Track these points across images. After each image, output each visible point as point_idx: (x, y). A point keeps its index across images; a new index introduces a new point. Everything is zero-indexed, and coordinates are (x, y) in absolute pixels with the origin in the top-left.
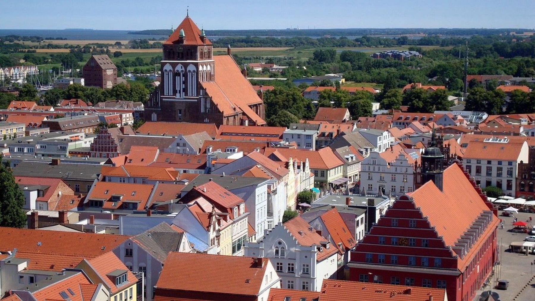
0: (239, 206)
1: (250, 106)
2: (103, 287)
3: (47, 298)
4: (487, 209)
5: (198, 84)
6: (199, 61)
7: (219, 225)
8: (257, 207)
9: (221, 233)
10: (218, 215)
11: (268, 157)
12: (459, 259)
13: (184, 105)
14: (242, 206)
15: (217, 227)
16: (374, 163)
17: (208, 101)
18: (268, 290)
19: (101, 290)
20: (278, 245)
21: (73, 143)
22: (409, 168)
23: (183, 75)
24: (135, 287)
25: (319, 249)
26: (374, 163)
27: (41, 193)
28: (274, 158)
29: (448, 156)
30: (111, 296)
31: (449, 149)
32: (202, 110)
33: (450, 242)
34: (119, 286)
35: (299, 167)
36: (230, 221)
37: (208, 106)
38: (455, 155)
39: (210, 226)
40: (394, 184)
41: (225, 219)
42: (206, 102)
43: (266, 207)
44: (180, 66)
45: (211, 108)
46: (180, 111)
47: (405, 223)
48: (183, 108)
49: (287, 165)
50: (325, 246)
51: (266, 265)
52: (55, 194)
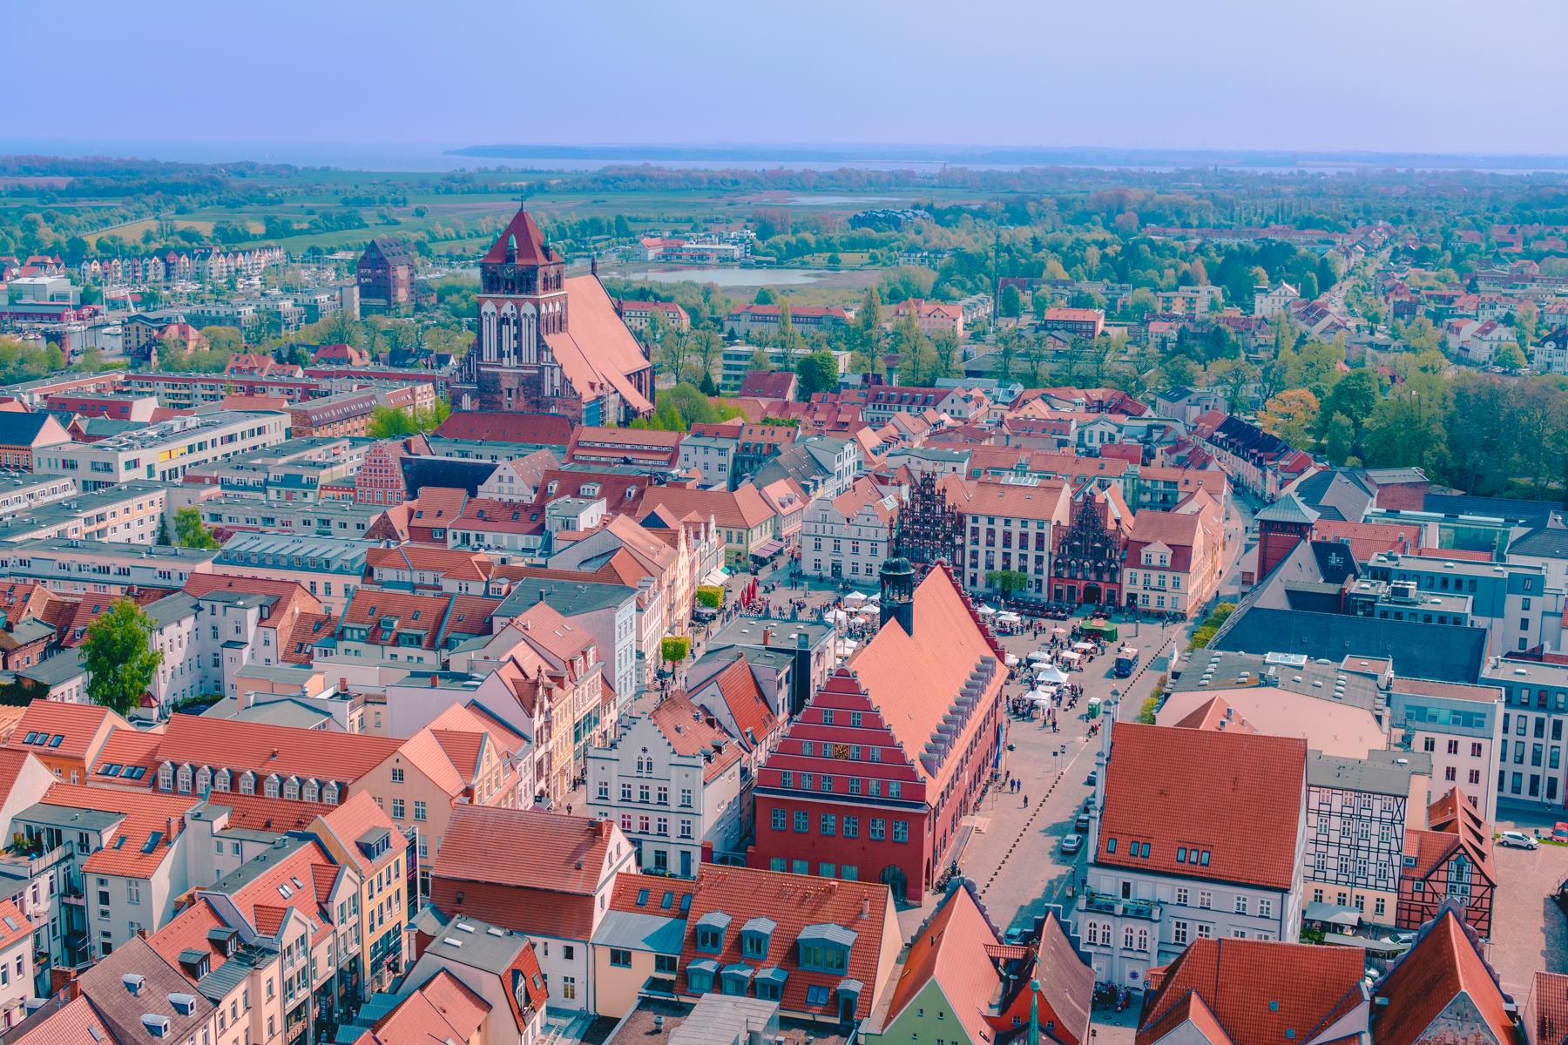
0: (584, 654)
1: (628, 377)
2: (348, 871)
4: (989, 653)
5: (540, 339)
6: (542, 296)
7: (550, 699)
8: (617, 648)
9: (553, 713)
11: (642, 524)
12: (929, 779)
13: (516, 381)
14: (591, 653)
15: (547, 705)
16: (824, 521)
17: (557, 371)
18: (614, 878)
20: (641, 754)
21: (327, 471)
22: (880, 530)
23: (515, 323)
25: (708, 759)
26: (824, 521)
27: (266, 611)
28: (653, 522)
29: (943, 508)
30: (362, 882)
31: (944, 497)
32: (547, 392)
33: (913, 752)
35: (697, 535)
36: (568, 685)
37: (557, 383)
38: (954, 507)
39: (534, 706)
40: (855, 559)
41: (561, 686)
43: (634, 642)
44: (508, 305)
45: (562, 386)
46: (510, 390)
49: (673, 542)
50: (718, 749)
51: (609, 834)
52: (288, 611)
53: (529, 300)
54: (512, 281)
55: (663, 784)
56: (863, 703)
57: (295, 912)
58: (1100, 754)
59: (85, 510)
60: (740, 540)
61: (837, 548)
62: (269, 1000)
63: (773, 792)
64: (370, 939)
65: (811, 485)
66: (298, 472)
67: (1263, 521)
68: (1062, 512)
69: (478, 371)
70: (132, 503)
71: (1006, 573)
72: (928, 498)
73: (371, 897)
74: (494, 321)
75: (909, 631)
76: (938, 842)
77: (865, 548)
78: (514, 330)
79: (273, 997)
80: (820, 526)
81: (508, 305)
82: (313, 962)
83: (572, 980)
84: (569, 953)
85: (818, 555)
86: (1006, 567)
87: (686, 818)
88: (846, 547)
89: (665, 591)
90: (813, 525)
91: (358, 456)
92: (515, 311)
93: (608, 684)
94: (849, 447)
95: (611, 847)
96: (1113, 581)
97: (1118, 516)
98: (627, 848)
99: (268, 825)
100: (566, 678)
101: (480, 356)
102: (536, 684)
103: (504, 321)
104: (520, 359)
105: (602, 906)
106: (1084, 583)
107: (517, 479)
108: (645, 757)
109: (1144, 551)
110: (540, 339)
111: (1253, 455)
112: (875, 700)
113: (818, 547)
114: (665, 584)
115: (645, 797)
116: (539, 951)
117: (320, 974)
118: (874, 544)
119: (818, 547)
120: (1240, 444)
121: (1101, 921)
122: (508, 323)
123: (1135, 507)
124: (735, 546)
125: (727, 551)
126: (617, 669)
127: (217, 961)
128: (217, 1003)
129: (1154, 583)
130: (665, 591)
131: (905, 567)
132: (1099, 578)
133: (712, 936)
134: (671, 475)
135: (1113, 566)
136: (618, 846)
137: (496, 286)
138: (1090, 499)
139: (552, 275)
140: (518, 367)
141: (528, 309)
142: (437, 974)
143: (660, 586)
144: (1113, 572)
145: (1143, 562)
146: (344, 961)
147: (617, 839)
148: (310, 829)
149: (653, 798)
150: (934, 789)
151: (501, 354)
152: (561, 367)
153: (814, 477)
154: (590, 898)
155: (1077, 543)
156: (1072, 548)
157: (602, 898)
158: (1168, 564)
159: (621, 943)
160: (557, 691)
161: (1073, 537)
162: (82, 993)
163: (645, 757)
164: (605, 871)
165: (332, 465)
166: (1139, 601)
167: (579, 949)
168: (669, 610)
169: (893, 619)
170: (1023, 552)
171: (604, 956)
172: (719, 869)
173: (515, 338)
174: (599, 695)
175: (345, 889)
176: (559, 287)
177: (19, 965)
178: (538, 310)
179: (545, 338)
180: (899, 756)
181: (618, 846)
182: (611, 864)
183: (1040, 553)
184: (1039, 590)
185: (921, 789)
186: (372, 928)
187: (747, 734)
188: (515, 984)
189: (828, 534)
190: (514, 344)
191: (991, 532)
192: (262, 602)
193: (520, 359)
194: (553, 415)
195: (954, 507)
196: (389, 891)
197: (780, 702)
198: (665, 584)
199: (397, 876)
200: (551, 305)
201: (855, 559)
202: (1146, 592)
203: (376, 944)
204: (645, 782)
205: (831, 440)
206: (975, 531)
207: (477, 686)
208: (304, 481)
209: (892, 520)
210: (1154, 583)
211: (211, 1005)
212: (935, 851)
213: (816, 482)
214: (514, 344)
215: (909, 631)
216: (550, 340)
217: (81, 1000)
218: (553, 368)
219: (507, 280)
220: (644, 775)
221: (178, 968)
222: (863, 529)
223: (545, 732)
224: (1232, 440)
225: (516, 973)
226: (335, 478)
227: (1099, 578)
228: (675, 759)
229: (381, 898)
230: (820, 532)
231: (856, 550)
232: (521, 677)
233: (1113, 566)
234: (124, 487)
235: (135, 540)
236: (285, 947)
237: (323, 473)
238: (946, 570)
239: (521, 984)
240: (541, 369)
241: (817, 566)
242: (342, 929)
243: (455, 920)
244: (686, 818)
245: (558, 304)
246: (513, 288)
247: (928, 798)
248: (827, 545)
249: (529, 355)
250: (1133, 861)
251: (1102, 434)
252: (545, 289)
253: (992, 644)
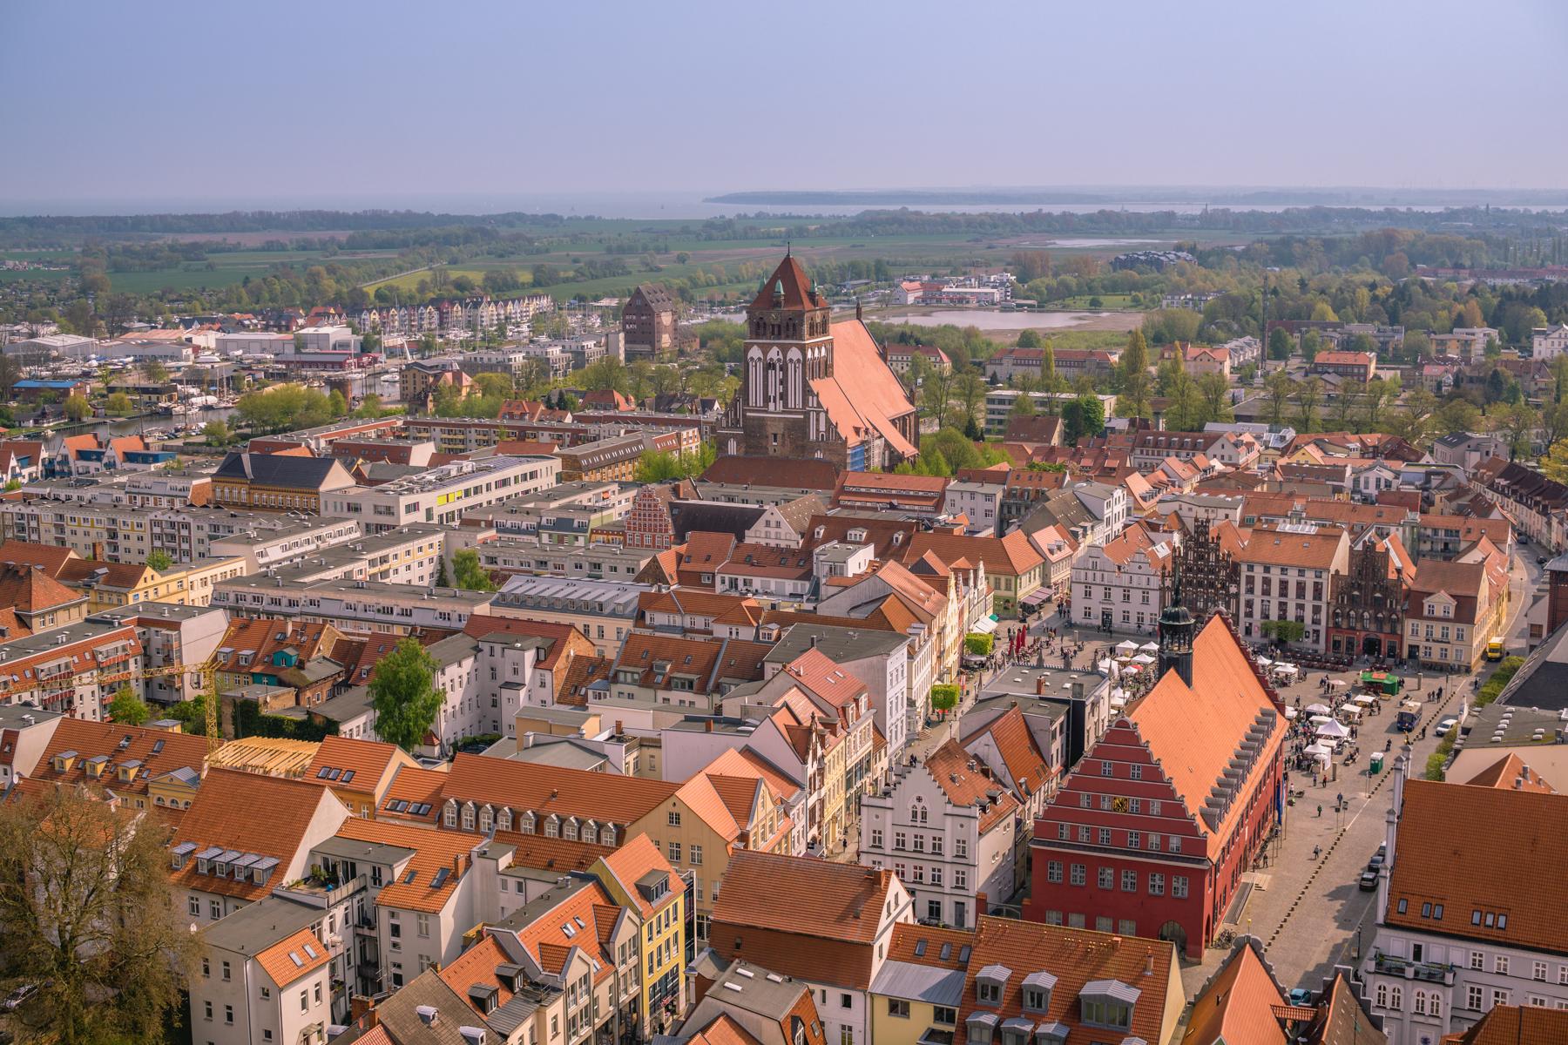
0: (856, 701)
1: (893, 422)
2: (629, 912)
3: (541, 940)
4: (1270, 706)
5: (805, 385)
7: (823, 746)
8: (889, 695)
9: (826, 760)
10: (822, 724)
14: (863, 700)
15: (819, 752)
17: (822, 416)
19: (626, 919)
20: (916, 803)
21: (598, 515)
22: (1152, 578)
24: (680, 900)
25: (984, 809)
27: (542, 652)
28: (922, 569)
29: (1217, 557)
30: (642, 924)
31: (1218, 545)
32: (813, 436)
33: (1194, 805)
34: (655, 904)
35: (966, 582)
36: (841, 733)
37: (822, 428)
38: (1229, 555)
39: (807, 753)
40: (1126, 607)
41: (834, 733)
42: (818, 420)
43: (905, 690)
44: (775, 349)
45: (827, 430)
46: (775, 435)
47: (1121, 772)
48: (779, 429)
49: (943, 587)
50: (993, 800)
51: (887, 884)
52: (564, 654)
54: (779, 326)
55: (938, 834)
56: (1144, 755)
57: (579, 952)
58: (1391, 812)
59: (369, 552)
60: (1008, 588)
61: (1107, 596)
62: (554, 1037)
63: (1050, 844)
64: (649, 980)
65: (1080, 531)
66: (571, 517)
67: (1553, 572)
68: (1340, 560)
69: (744, 416)
70: (413, 546)
71: (1282, 623)
72: (1202, 545)
73: (650, 939)
74: (760, 366)
75: (1188, 682)
76: (1218, 899)
77: (1136, 596)
78: (780, 375)
79: (557, 1034)
80: (1090, 574)
81: (775, 349)
82: (595, 1001)
83: (850, 1029)
84: (847, 1002)
85: (1088, 603)
86: (1283, 617)
87: (961, 868)
88: (1117, 595)
89: (934, 638)
90: (1083, 572)
91: (627, 500)
92: (781, 356)
93: (879, 731)
94: (1118, 493)
95: (890, 897)
96: (1393, 632)
97: (1399, 565)
98: (905, 898)
99: (550, 866)
100: (839, 725)
101: (746, 401)
102: (809, 731)
103: (770, 366)
104: (785, 405)
105: (881, 957)
106: (1363, 634)
107: (784, 522)
108: (919, 806)
109: (1427, 602)
110: (805, 385)
111: (1537, 503)
112: (1156, 752)
113: (1088, 594)
114: (935, 631)
115: (919, 846)
116: (817, 998)
117: (601, 1014)
118: (1145, 591)
119: (1088, 594)
120: (1524, 491)
121: (1391, 984)
122: (774, 368)
123: (1416, 555)
124: (1003, 593)
125: (995, 598)
126: (888, 716)
127: (504, 996)
128: (505, 1037)
129: (1437, 634)
130: (934, 638)
131: (1185, 617)
132: (1380, 630)
133: (993, 989)
134: (938, 521)
135: (1394, 617)
136: (897, 895)
137: (762, 330)
138: (1370, 548)
139: (818, 320)
140: (783, 412)
141: (794, 354)
142: (718, 1018)
143: (930, 633)
144: (1394, 623)
145: (1426, 613)
146: (624, 998)
147: (895, 887)
148: (592, 870)
149: (928, 848)
150: (1216, 843)
151: (767, 399)
152: (827, 412)
153: (1082, 524)
154: (871, 947)
155: (1356, 593)
156: (1352, 599)
157: (881, 947)
158: (1452, 615)
159: (899, 993)
160: (830, 738)
161: (1352, 586)
162: (380, 1022)
163: (919, 806)
164: (884, 921)
165: (602, 509)
166: (1421, 654)
167: (857, 998)
168: (939, 657)
169: (1172, 670)
170: (1300, 601)
171: (882, 1006)
172: (1002, 922)
173: (781, 383)
174: (871, 743)
175: (626, 931)
176: (825, 332)
177: (317, 992)
178: (804, 355)
179: (811, 382)
180: (1179, 810)
181: (897, 895)
182: (889, 914)
183: (1317, 603)
184: (1317, 641)
185: (1202, 844)
186: (651, 970)
187: (1021, 785)
188: (794, 1030)
189: (1098, 581)
190: (780, 389)
191: (1267, 581)
192: (539, 645)
193: (785, 405)
194: (819, 460)
195: (1229, 555)
196: (668, 933)
197: (1054, 752)
198: (935, 631)
199: (675, 919)
200: (816, 351)
201: (1126, 607)
202: (1428, 644)
203: (654, 985)
204: (920, 832)
205: (1098, 487)
206: (1250, 580)
207: (751, 732)
208: (576, 524)
209: (1164, 568)
210: (1437, 634)
211: (499, 1038)
212: (1215, 908)
213: (1085, 529)
214: (780, 389)
215: (1188, 682)
216: (815, 384)
217: (378, 1030)
218: (818, 413)
220: (919, 824)
221: (468, 1002)
222: (1134, 577)
223: (818, 778)
224: (1515, 487)
225: (795, 1020)
226: (605, 522)
227: (1380, 630)
228: (949, 809)
229: (659, 940)
230: (1090, 580)
231: (1127, 598)
232: (794, 723)
233: (1394, 617)
234: (405, 530)
235: (415, 582)
236: (569, 985)
237: (594, 517)
238: (1225, 621)
239: (800, 1031)
240: (807, 414)
241: (1087, 614)
242: (622, 969)
243: (734, 964)
244: (961, 868)
245: (823, 350)
246: (779, 334)
247: (1209, 854)
248: (1098, 592)
249: (795, 400)
250: (1424, 925)
251: (1378, 480)
252: (811, 334)
253: (1272, 697)
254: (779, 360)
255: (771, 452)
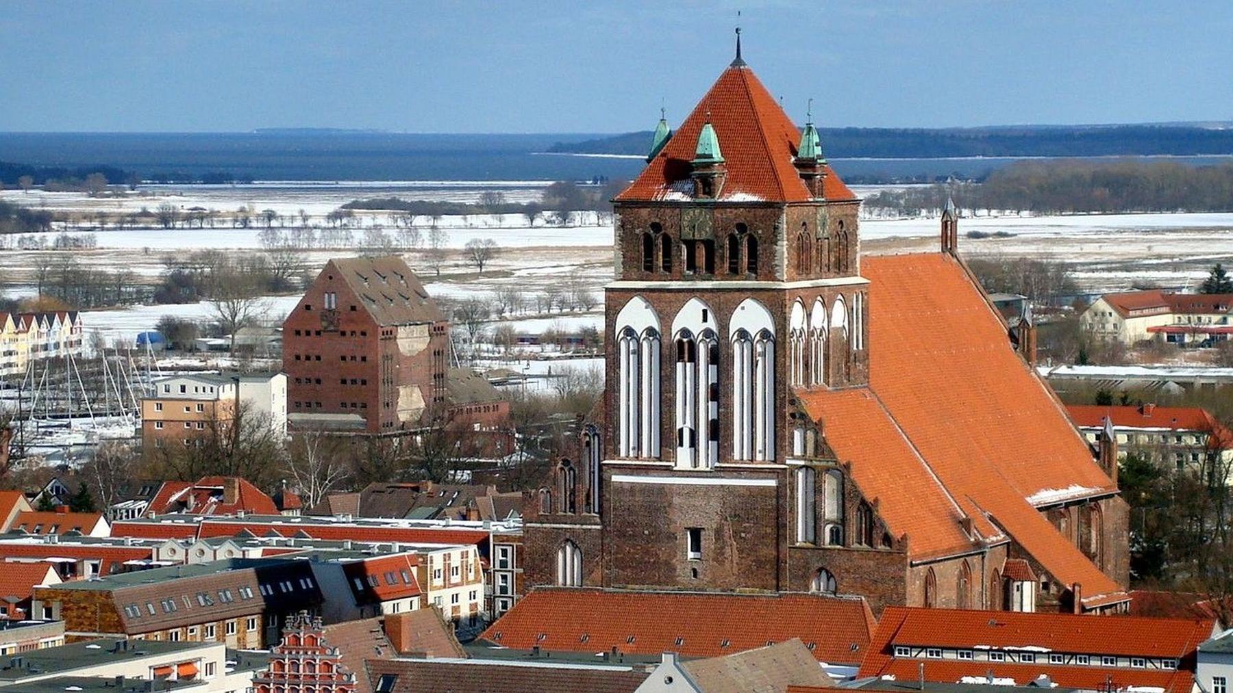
13: (715, 504)
42: (818, 490)
46: (696, 534)
53: (755, 293)
54: (709, 244)
92: (712, 324)
104: (724, 452)
122: (693, 358)
176: (842, 266)
178: (781, 318)
193: (724, 452)
200: (818, 310)
214: (707, 410)
219: (691, 245)
240: (785, 477)
252: (803, 267)
254: (708, 333)
255: (683, 575)
